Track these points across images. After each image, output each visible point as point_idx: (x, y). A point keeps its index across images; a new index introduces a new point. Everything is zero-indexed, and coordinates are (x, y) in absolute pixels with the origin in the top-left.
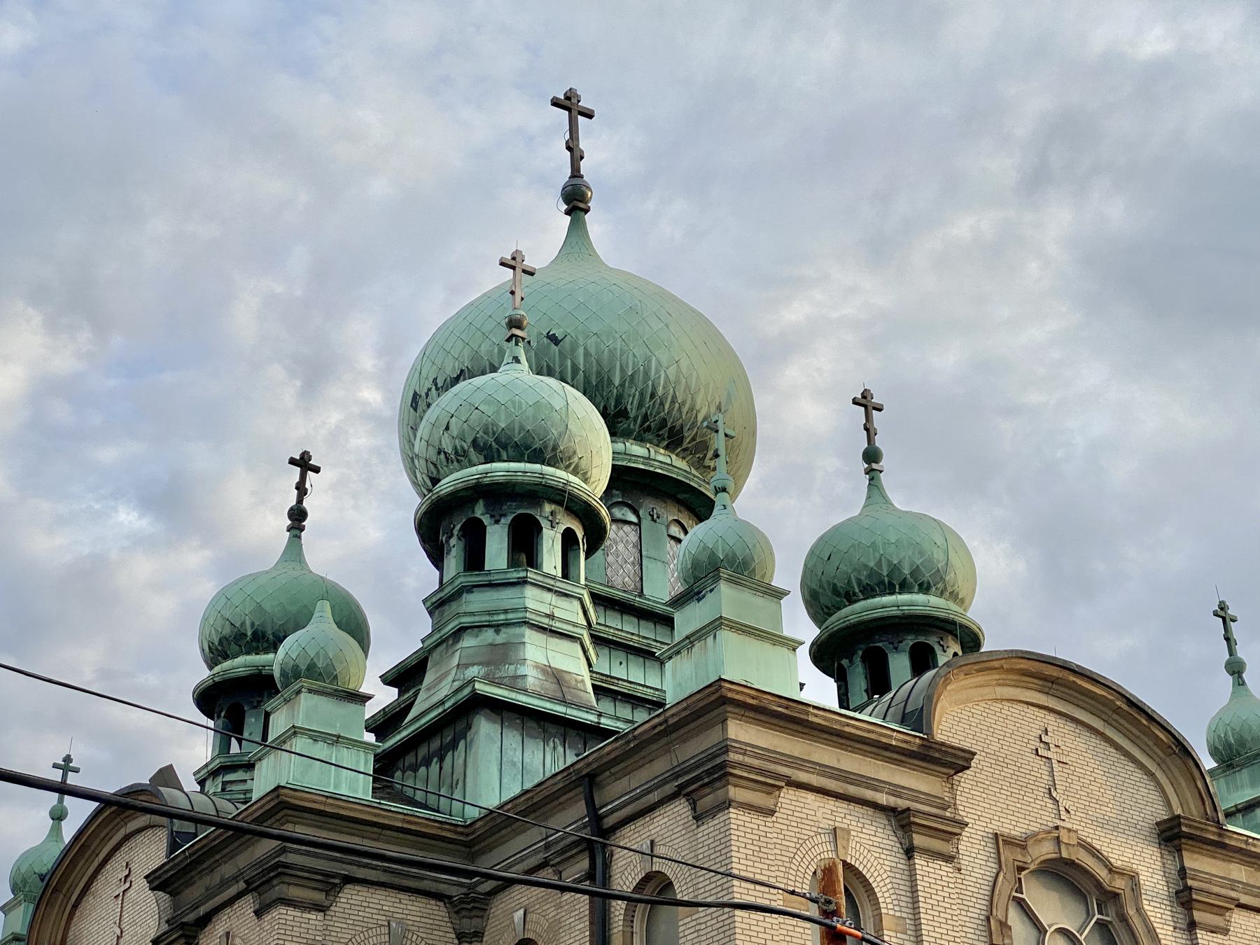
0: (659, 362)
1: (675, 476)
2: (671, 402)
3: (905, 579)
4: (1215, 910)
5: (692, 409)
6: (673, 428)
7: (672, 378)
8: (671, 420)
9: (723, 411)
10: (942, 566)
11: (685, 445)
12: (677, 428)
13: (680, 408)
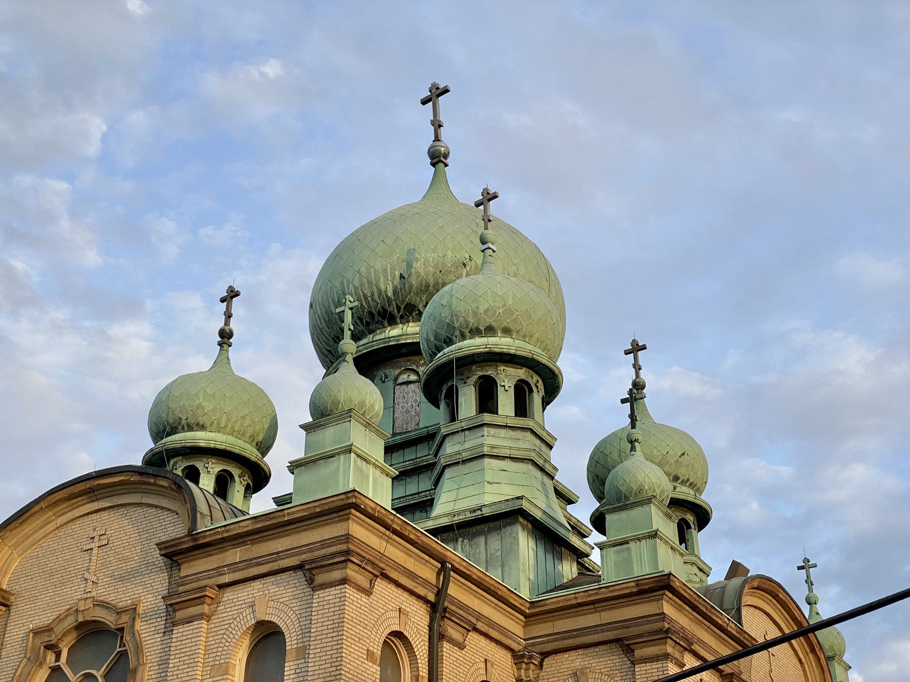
0: (348, 281)
1: (376, 347)
2: (365, 299)
3: (435, 344)
4: (198, 601)
5: (380, 293)
6: (379, 313)
7: (357, 284)
8: (374, 309)
9: (406, 277)
10: (450, 321)
11: (398, 316)
12: (381, 311)
13: (372, 299)
